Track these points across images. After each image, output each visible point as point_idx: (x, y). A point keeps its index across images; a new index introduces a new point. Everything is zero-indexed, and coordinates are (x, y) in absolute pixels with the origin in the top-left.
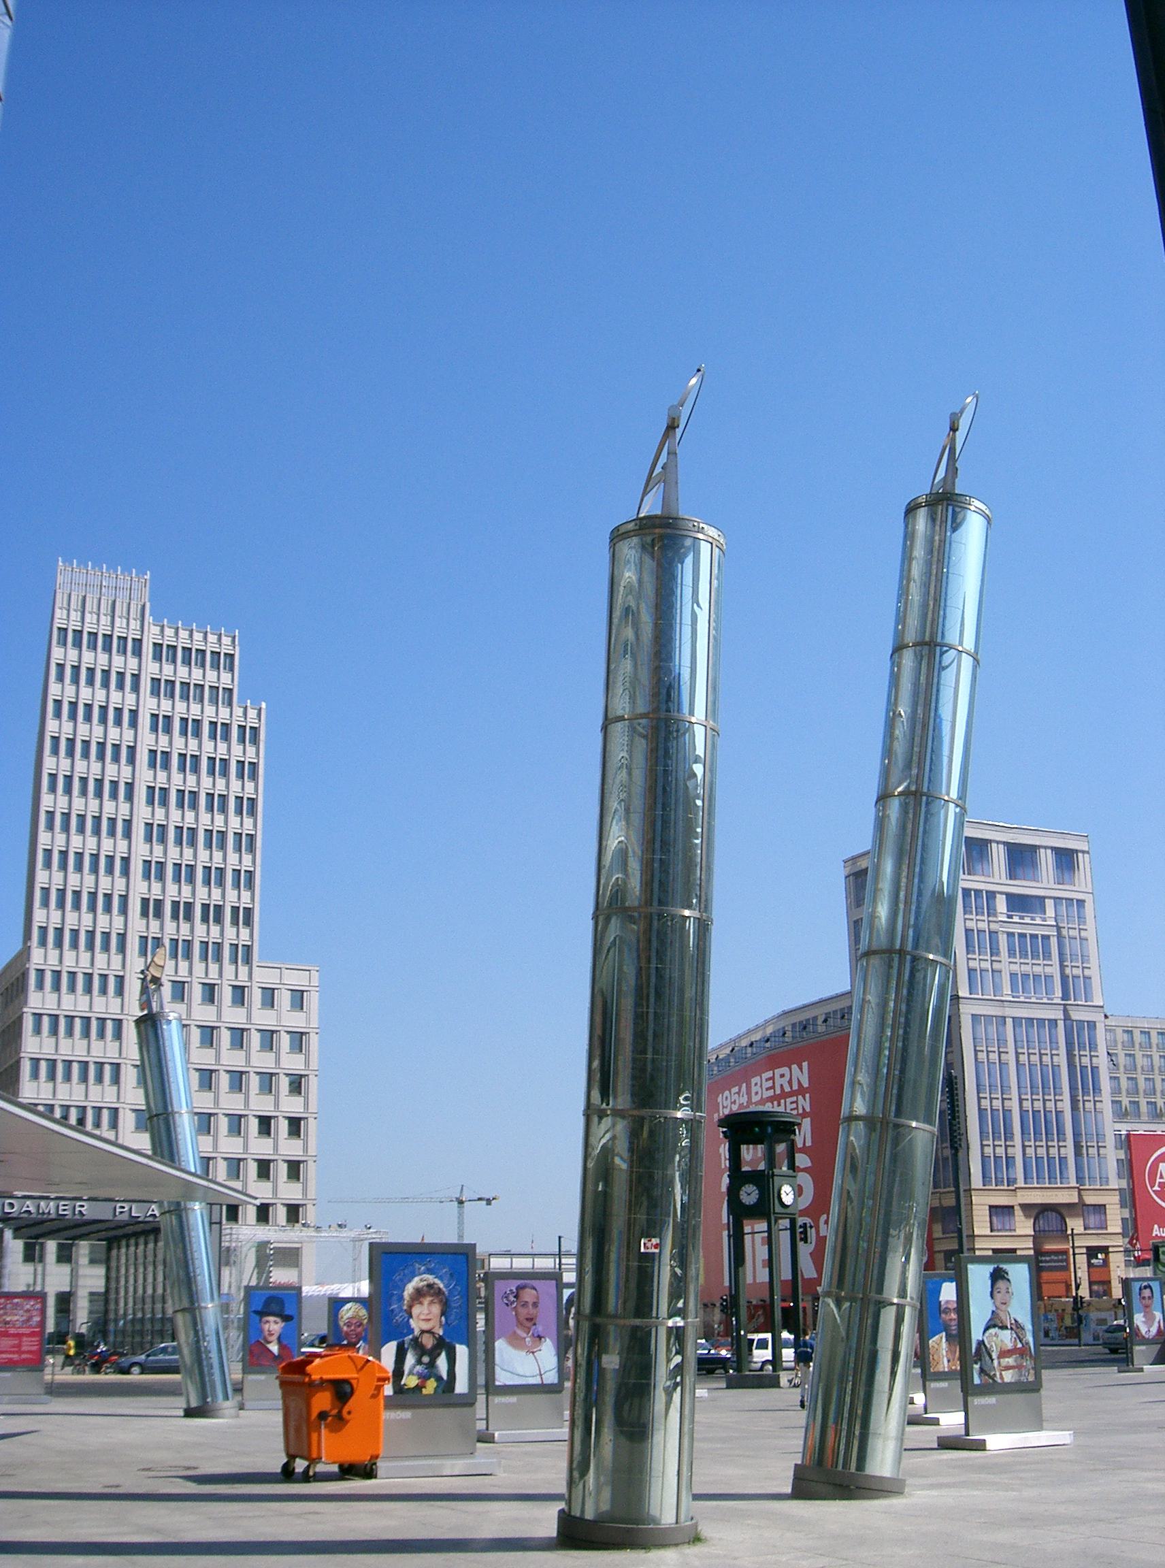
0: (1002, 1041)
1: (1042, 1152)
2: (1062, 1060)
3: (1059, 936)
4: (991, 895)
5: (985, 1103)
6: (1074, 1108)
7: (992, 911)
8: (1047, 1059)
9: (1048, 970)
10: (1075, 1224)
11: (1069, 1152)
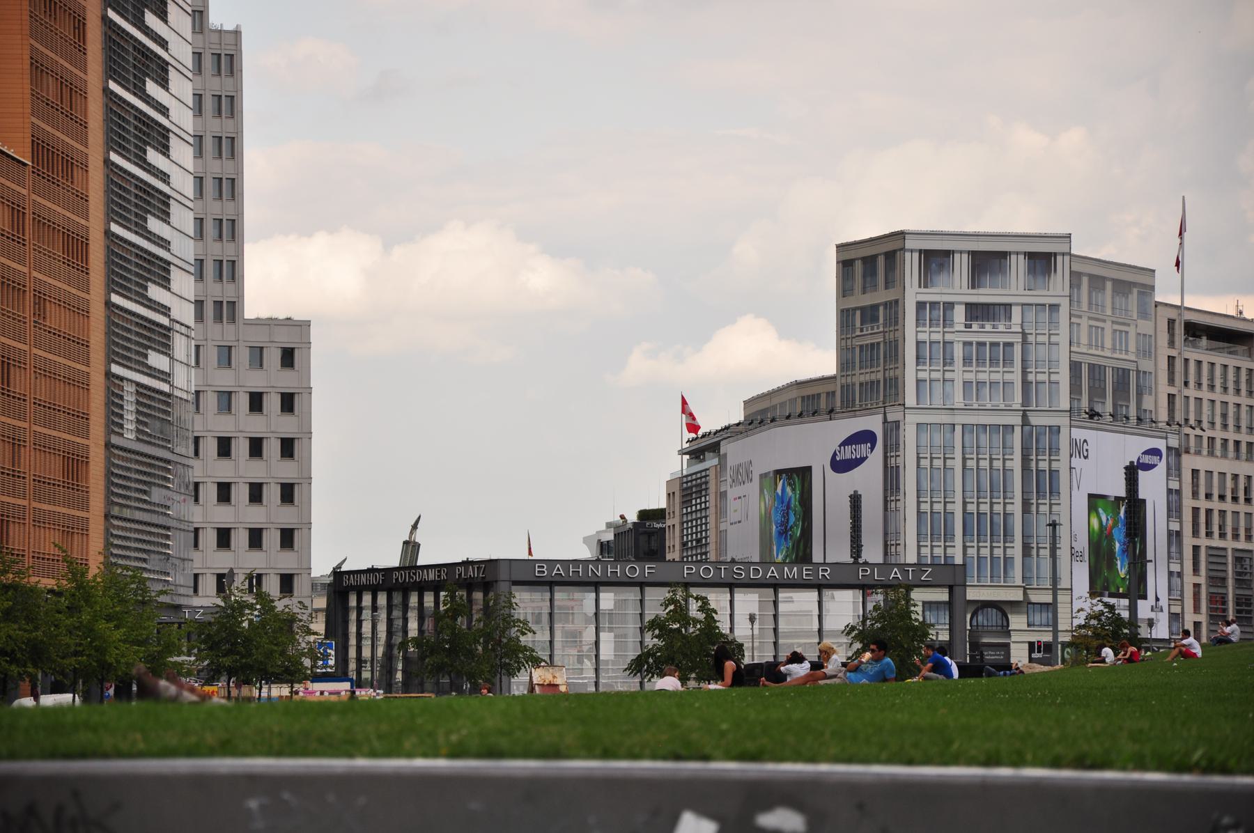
0: (948, 448)
1: (985, 552)
3: (1025, 342)
4: (949, 306)
5: (925, 507)
8: (998, 464)
9: (1008, 377)
10: (1017, 622)
11: (1016, 551)
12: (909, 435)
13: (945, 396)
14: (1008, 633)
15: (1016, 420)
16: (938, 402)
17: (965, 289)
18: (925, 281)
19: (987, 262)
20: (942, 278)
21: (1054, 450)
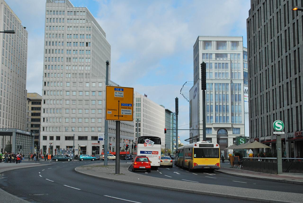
1: (221, 115)
3: (231, 63)
4: (211, 54)
9: (227, 71)
10: (230, 132)
11: (230, 115)
14: (227, 136)
18: (205, 48)
19: (220, 44)
20: (209, 47)
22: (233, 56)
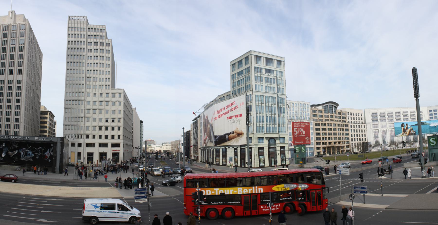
0: (262, 101)
1: (271, 126)
2: (276, 106)
3: (277, 79)
4: (261, 69)
5: (258, 115)
6: (279, 116)
7: (261, 72)
8: (273, 105)
9: (274, 86)
10: (278, 142)
11: (277, 126)
12: (253, 97)
13: (261, 89)
14: (276, 144)
15: (276, 96)
16: (260, 90)
17: (264, 65)
18: (256, 63)
19: (269, 60)
20: (259, 62)
21: (283, 103)
22: (278, 73)
